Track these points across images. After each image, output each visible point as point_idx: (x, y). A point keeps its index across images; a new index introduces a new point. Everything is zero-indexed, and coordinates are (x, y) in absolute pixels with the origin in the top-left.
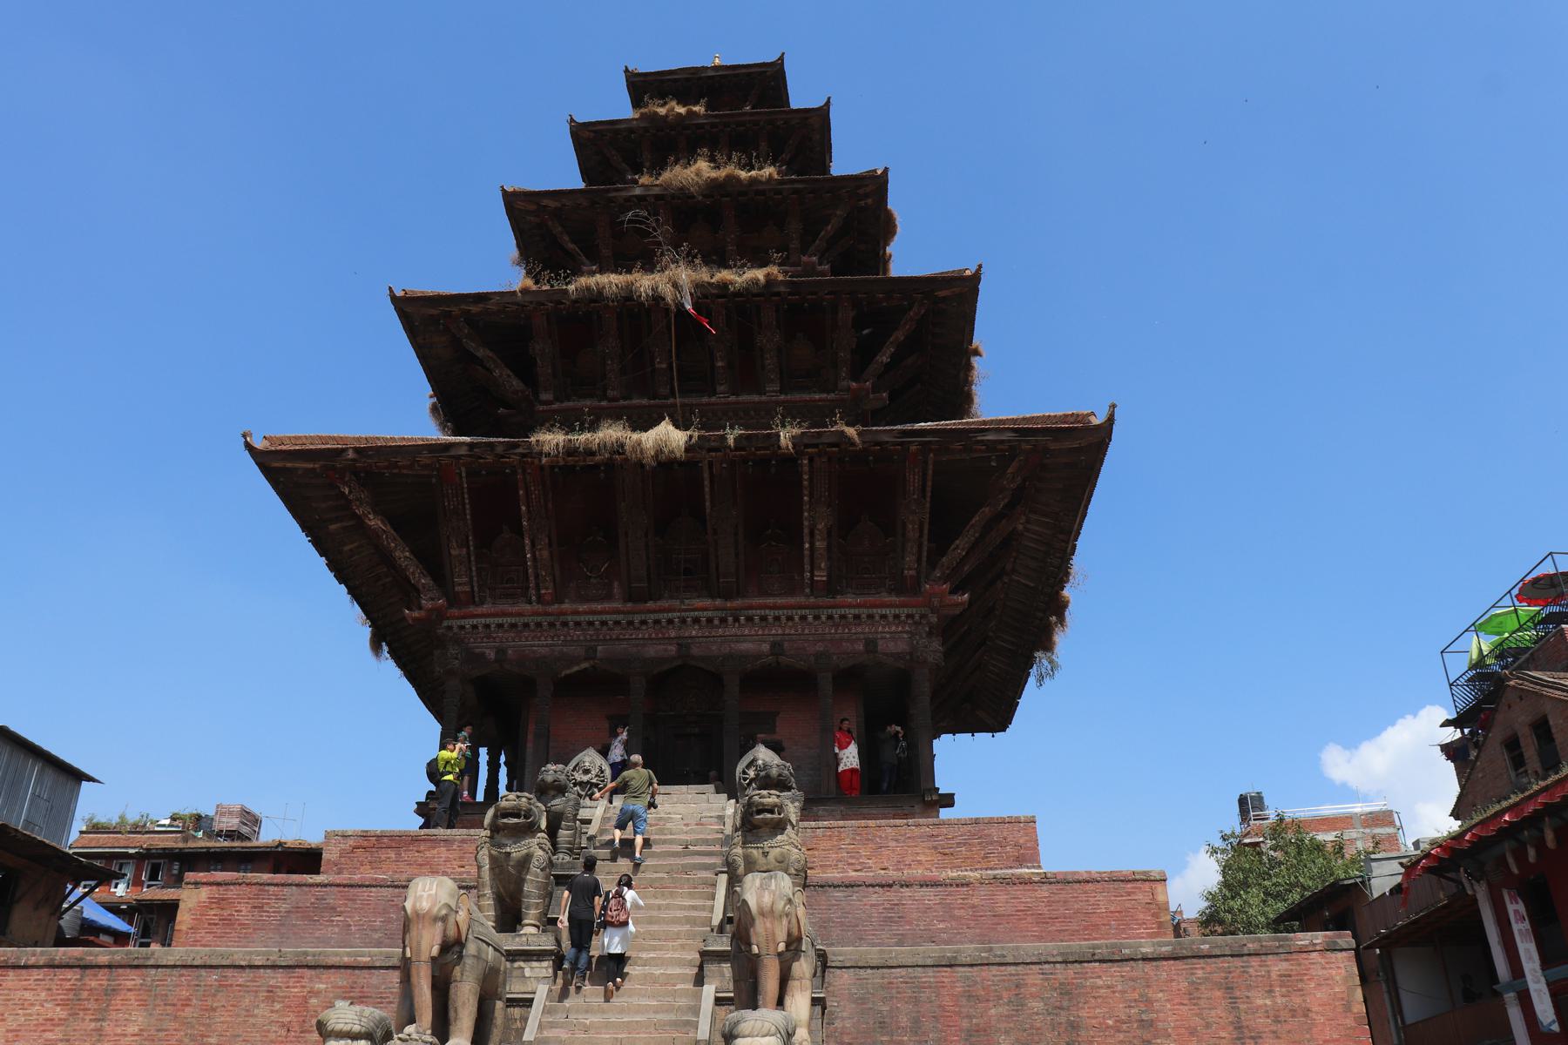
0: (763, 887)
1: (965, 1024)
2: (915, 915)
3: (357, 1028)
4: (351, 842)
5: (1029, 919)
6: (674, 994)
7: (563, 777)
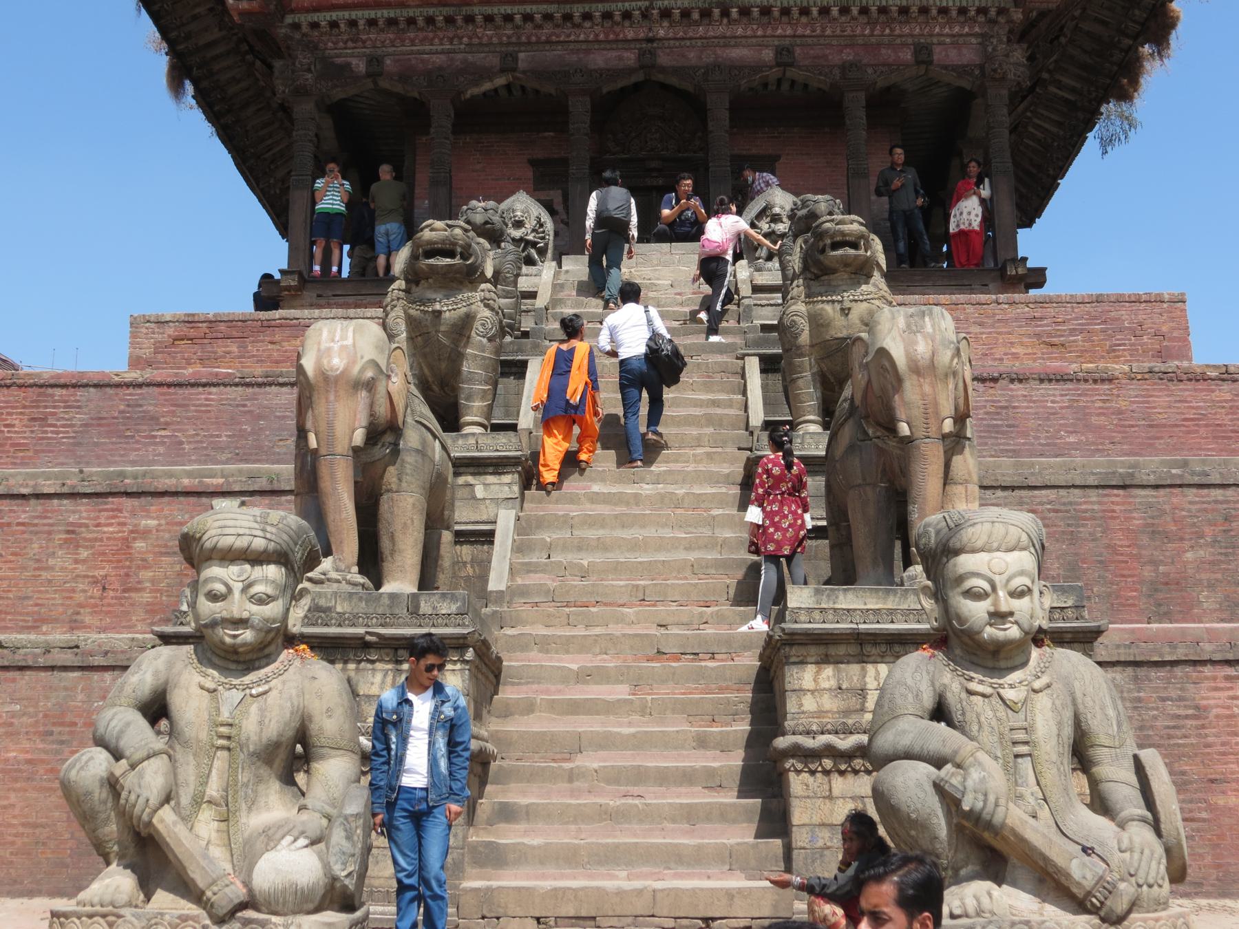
0: (912, 329)
1: (1148, 572)
2: (1032, 424)
3: (259, 544)
4: (170, 331)
5: (1202, 431)
6: (713, 522)
7: (496, 219)
